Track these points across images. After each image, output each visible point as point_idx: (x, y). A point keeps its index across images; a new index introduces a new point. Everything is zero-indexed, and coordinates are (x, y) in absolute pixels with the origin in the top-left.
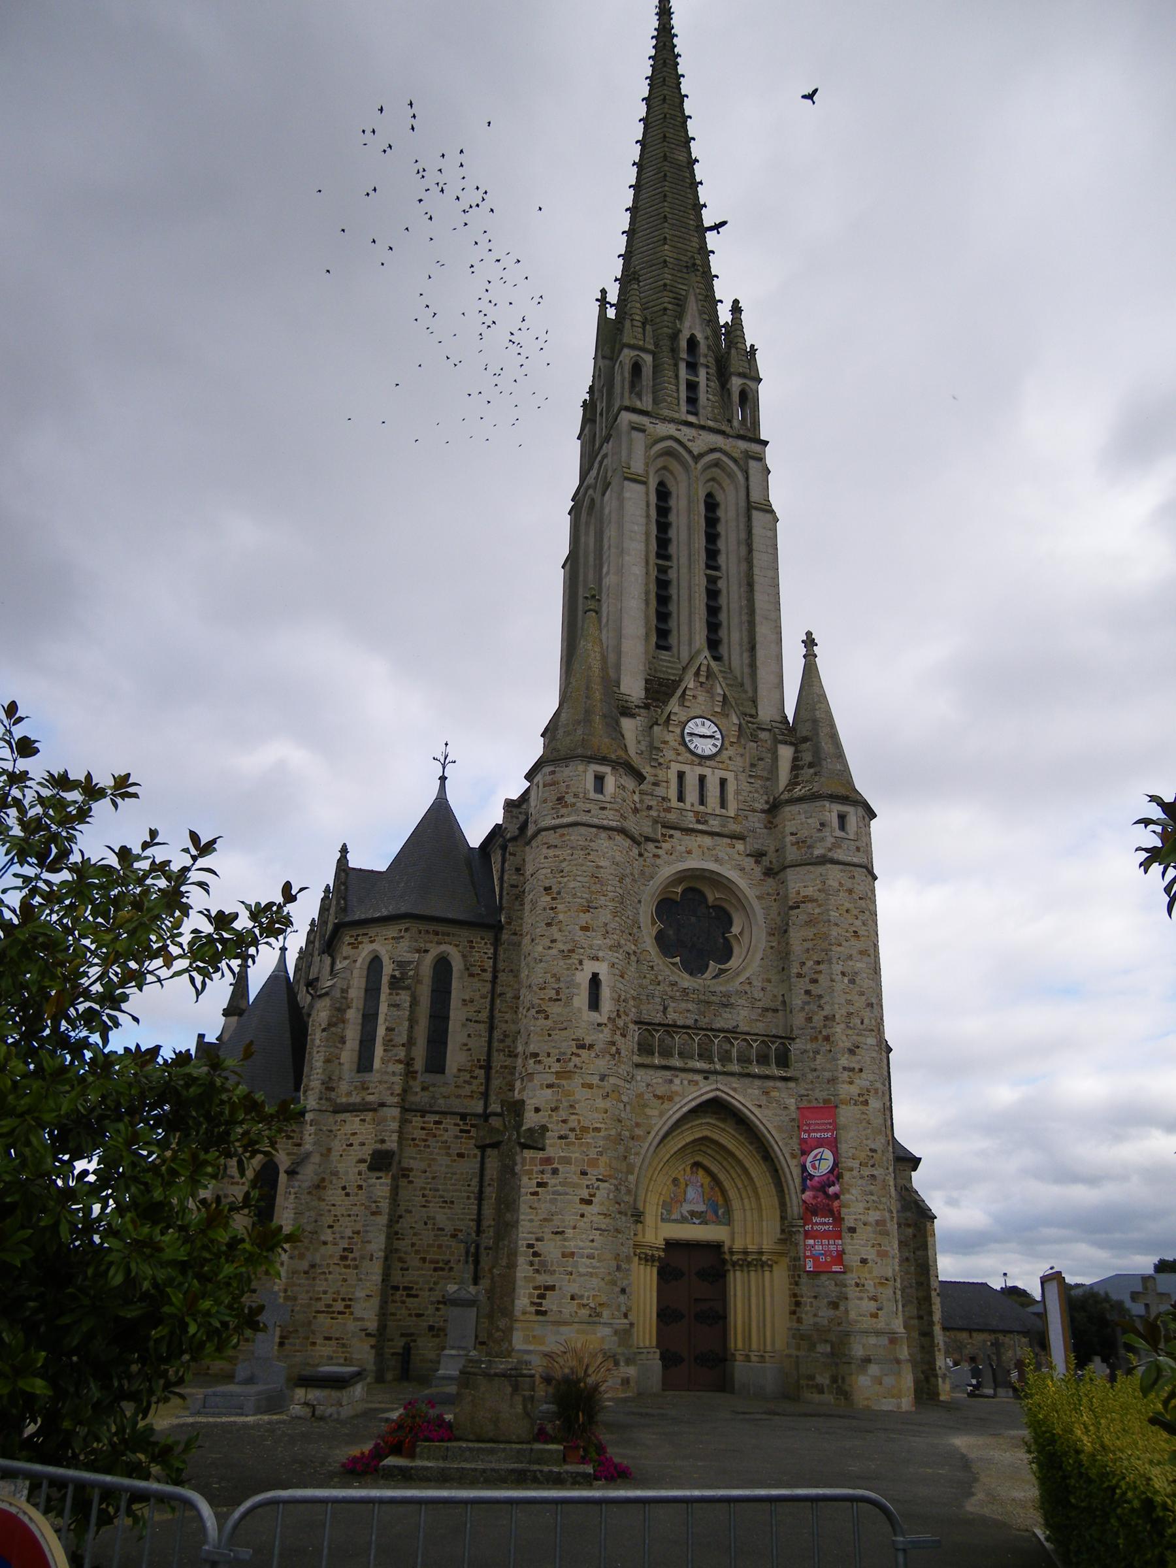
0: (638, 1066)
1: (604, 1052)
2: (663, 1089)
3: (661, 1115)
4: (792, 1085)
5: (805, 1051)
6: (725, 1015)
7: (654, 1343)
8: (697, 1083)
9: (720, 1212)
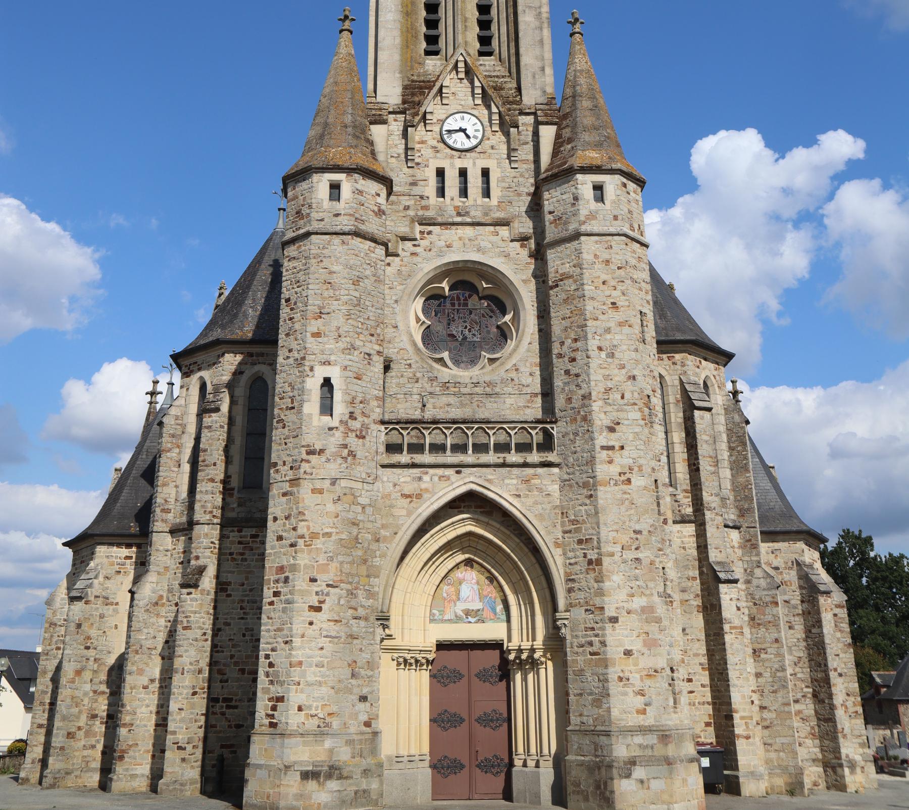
4: (556, 470)
6: (489, 405)
8: (448, 478)
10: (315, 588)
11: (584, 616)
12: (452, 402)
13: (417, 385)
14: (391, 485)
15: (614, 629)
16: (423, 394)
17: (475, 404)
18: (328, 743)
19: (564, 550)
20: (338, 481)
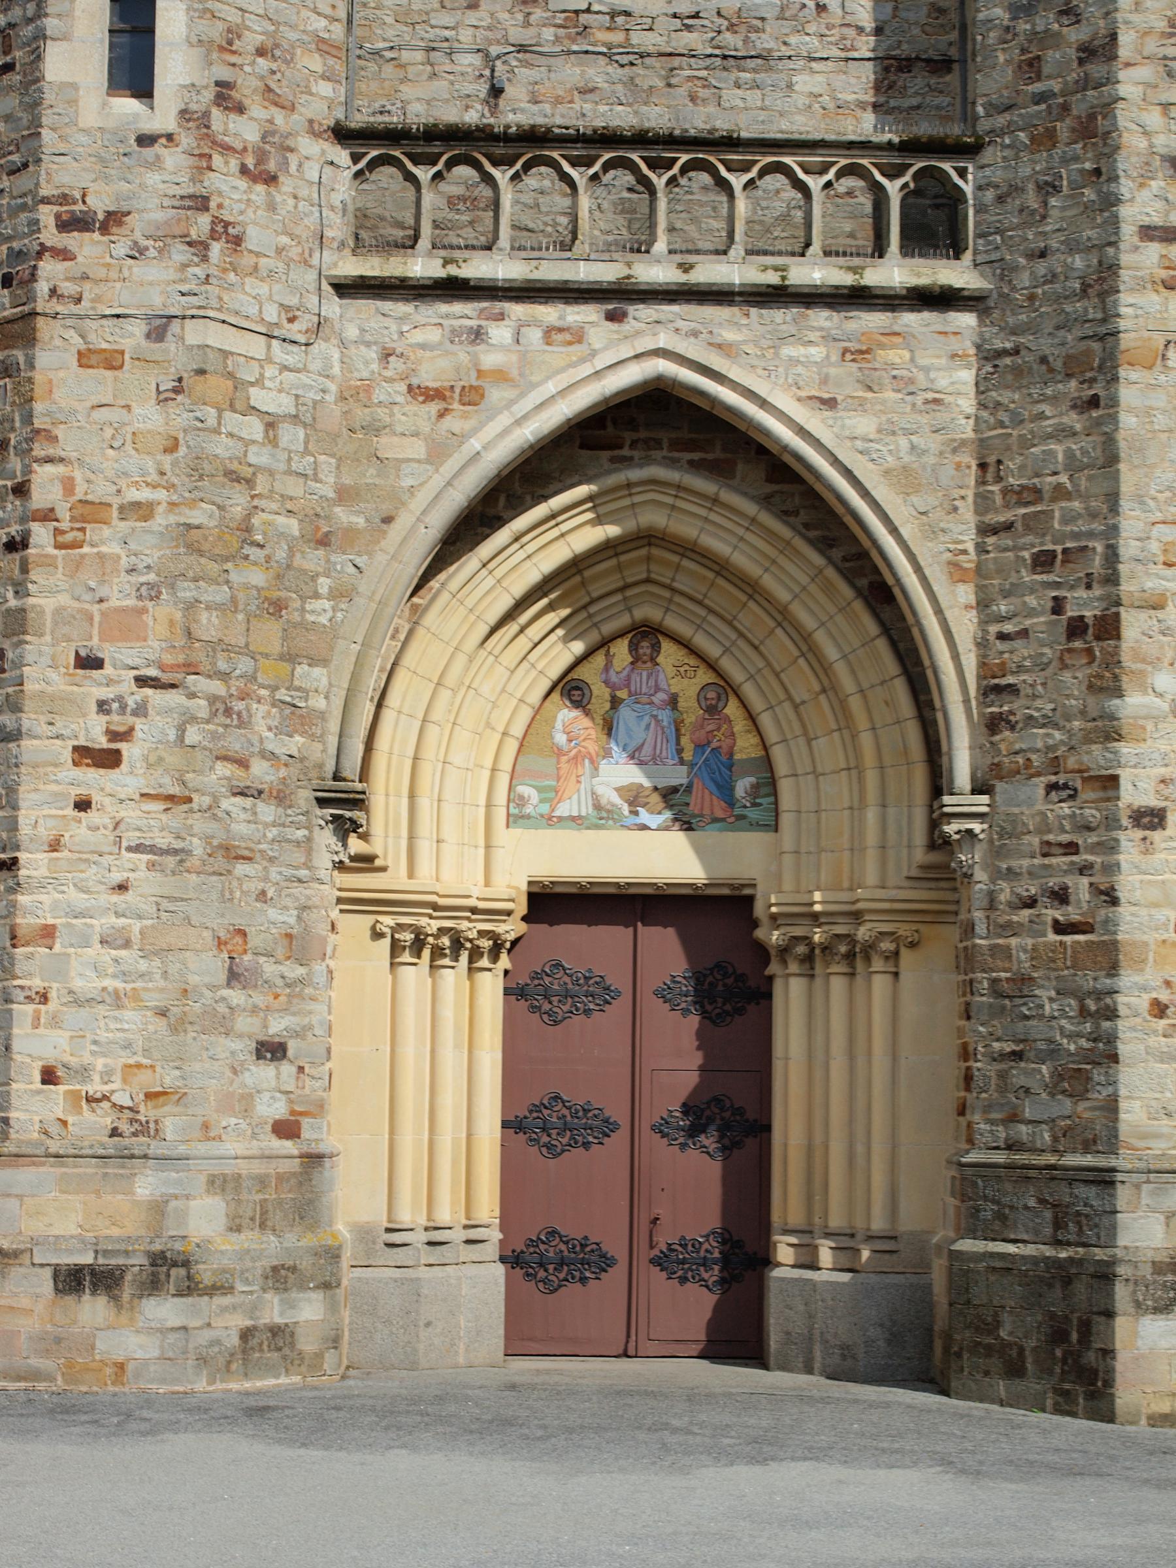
0: (347, 288)
1: (163, 238)
2: (444, 363)
3: (437, 454)
4: (966, 320)
5: (1015, 189)
6: (732, 96)
7: (488, 1207)
8: (577, 336)
9: (742, 786)
10: (94, 687)
11: (1040, 806)
12: (600, 81)
13: (472, 17)
14: (373, 354)
15: (1147, 847)
16: (494, 50)
17: (682, 91)
18: (147, 1185)
19: (980, 589)
20: (175, 326)
